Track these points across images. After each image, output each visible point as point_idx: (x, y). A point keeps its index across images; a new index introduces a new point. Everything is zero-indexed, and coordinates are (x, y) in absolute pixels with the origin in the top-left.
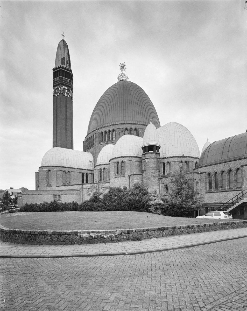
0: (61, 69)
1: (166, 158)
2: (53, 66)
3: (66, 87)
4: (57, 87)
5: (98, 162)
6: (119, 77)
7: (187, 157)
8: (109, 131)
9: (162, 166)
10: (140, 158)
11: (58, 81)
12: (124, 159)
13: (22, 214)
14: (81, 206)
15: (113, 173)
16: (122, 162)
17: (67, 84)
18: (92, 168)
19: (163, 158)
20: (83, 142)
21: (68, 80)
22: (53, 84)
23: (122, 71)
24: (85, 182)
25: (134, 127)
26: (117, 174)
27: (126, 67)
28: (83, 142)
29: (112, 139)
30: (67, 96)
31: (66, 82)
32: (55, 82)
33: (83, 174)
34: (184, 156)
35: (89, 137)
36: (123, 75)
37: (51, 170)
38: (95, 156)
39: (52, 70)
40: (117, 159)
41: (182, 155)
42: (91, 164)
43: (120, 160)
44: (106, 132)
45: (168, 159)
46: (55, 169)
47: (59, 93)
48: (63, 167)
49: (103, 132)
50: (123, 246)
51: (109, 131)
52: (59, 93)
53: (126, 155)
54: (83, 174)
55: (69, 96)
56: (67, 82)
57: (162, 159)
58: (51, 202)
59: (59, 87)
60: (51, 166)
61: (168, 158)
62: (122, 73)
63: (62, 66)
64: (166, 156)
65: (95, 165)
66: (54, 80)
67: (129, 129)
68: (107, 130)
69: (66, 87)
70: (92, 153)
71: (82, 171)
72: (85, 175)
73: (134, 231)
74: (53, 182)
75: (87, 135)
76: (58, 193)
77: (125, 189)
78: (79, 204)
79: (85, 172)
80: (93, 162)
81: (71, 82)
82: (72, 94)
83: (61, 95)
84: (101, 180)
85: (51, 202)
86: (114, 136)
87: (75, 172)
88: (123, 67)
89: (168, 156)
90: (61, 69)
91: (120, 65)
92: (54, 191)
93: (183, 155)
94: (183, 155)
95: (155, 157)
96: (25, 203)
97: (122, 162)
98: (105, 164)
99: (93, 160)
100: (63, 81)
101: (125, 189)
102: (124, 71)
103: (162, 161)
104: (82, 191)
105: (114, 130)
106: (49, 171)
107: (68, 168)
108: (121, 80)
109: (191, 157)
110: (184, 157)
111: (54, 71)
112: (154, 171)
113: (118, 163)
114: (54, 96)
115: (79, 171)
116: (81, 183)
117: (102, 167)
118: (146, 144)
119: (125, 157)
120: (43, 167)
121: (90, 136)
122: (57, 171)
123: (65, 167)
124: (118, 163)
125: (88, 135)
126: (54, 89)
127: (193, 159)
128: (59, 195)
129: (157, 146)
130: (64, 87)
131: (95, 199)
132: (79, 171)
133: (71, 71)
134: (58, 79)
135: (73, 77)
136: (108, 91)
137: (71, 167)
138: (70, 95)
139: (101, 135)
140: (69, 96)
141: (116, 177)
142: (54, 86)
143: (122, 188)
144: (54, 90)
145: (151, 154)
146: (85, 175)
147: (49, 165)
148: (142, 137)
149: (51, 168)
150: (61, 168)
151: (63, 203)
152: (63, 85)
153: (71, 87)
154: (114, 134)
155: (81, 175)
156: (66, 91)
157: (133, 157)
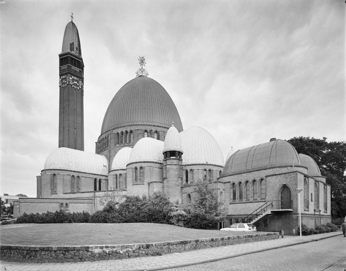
0: (70, 56)
1: (188, 165)
2: (60, 52)
3: (75, 78)
4: (64, 77)
5: (113, 167)
6: (137, 73)
7: (211, 165)
8: (127, 132)
9: (185, 174)
10: (161, 164)
11: (66, 69)
12: (143, 165)
13: (19, 227)
14: (93, 217)
15: (131, 179)
16: (141, 168)
17: (76, 74)
18: (106, 173)
19: (186, 165)
20: (96, 143)
21: (78, 70)
22: (60, 73)
23: (141, 66)
24: (98, 189)
25: (154, 129)
26: (135, 181)
27: (146, 61)
28: (96, 143)
29: (130, 141)
31: (75, 71)
32: (62, 70)
33: (95, 180)
34: (208, 163)
35: (103, 138)
36: (142, 70)
37: (56, 174)
38: (110, 159)
40: (135, 164)
41: (205, 163)
42: (105, 168)
43: (138, 166)
44: (122, 133)
45: (192, 166)
46: (61, 173)
47: (67, 84)
48: (71, 171)
49: (119, 133)
50: (142, 262)
51: (127, 132)
52: (67, 84)
53: (145, 161)
54: (95, 180)
55: (80, 88)
56: (77, 72)
57: (184, 166)
58: (57, 212)
59: (67, 76)
60: (57, 170)
61: (191, 165)
62: (141, 67)
63: (71, 52)
64: (189, 163)
65: (110, 170)
66: (60, 68)
67: (149, 131)
68: (124, 131)
69: (75, 78)
70: (106, 156)
71: (95, 177)
72: (98, 181)
73: (154, 245)
74: (60, 189)
75: (100, 135)
76: (64, 202)
77: (144, 198)
78: (91, 214)
79: (98, 178)
80: (107, 167)
81: (82, 72)
82: (82, 87)
83: (70, 86)
84: (117, 188)
85: (57, 212)
86: (132, 139)
87: (86, 177)
88: (142, 61)
89: (191, 163)
90: (70, 56)
91: (139, 58)
92: (61, 199)
93: (207, 162)
94: (207, 162)
95: (177, 164)
96: (24, 213)
97: (141, 168)
98: (121, 170)
99: (107, 164)
100: (72, 70)
101: (144, 198)
102: (143, 66)
103: (185, 168)
104: (94, 199)
105: (131, 132)
106: (54, 175)
107: (77, 172)
108: (140, 76)
109: (215, 165)
110: (208, 164)
111: (60, 58)
112: (176, 179)
113: (136, 168)
114: (60, 86)
115: (91, 176)
116: (93, 190)
117: (118, 173)
118: (167, 149)
119: (145, 162)
120: (47, 170)
121: (104, 136)
122: (64, 175)
123: (74, 172)
124: (136, 168)
125: (101, 135)
126: (60, 78)
127: (217, 167)
128: (67, 204)
129: (179, 152)
130: (73, 77)
131: (110, 209)
132: (91, 176)
133: (82, 60)
134: (65, 67)
135: (84, 67)
136: (125, 86)
137: (81, 171)
138: (81, 88)
139: (117, 136)
140: (79, 88)
141: (134, 184)
142: (60, 75)
143: (141, 197)
144: (61, 80)
145: (173, 161)
146: (98, 181)
147: (54, 168)
148: (163, 140)
149: (57, 171)
150: (68, 173)
151: (72, 213)
152: (72, 75)
153: (82, 79)
154: (132, 136)
155: (93, 181)
157: (153, 162)
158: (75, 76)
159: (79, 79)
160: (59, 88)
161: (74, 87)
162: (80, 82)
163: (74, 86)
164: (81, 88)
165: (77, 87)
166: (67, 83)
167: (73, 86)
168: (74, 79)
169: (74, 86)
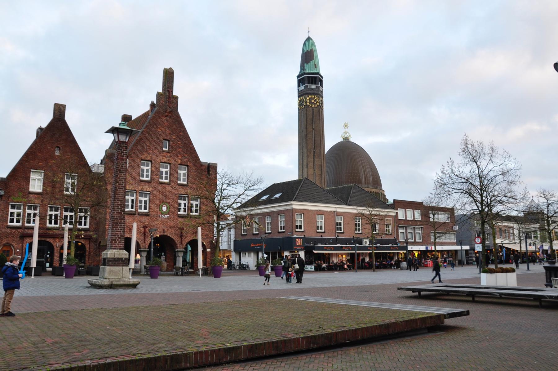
4: (301, 98)
21: (314, 86)
22: (298, 94)
32: (300, 91)
39: (297, 78)
47: (304, 106)
52: (304, 106)
59: (304, 97)
66: (298, 90)
111: (299, 79)
114: (299, 108)
126: (299, 100)
130: (310, 96)
135: (322, 78)
140: (316, 106)
142: (299, 97)
144: (299, 101)
156: (313, 101)
158: (311, 94)
160: (298, 109)
161: (311, 106)
166: (305, 104)
168: (311, 98)
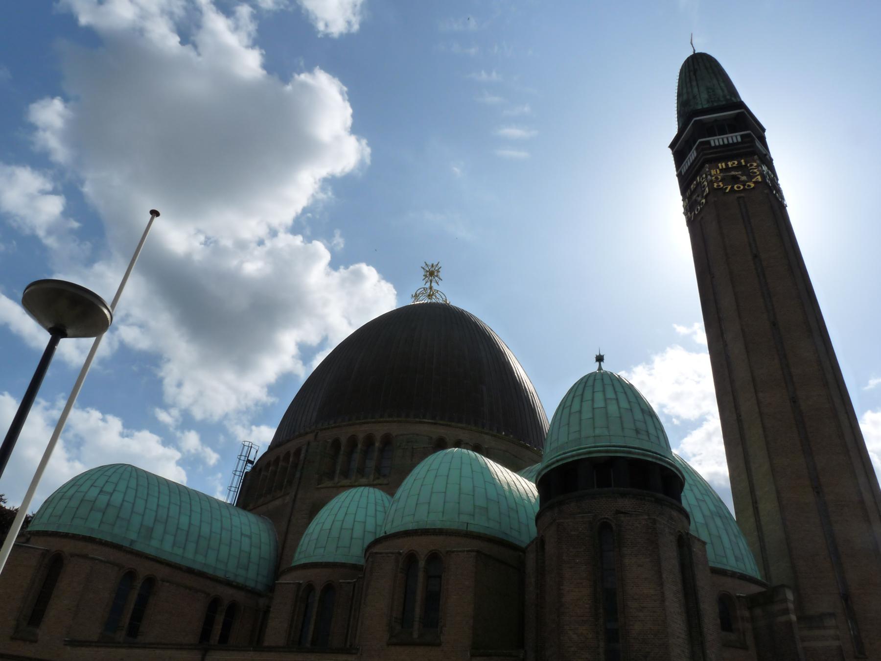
11: (696, 158)
21: (735, 137)
30: (744, 189)
55: (754, 183)
56: (734, 144)
100: (716, 147)
130: (722, 165)
135: (765, 130)
138: (760, 180)
140: (752, 185)
159: (745, 162)
162: (751, 165)
163: (732, 187)
164: (760, 180)
165: (744, 185)
167: (729, 187)
169: (732, 187)
